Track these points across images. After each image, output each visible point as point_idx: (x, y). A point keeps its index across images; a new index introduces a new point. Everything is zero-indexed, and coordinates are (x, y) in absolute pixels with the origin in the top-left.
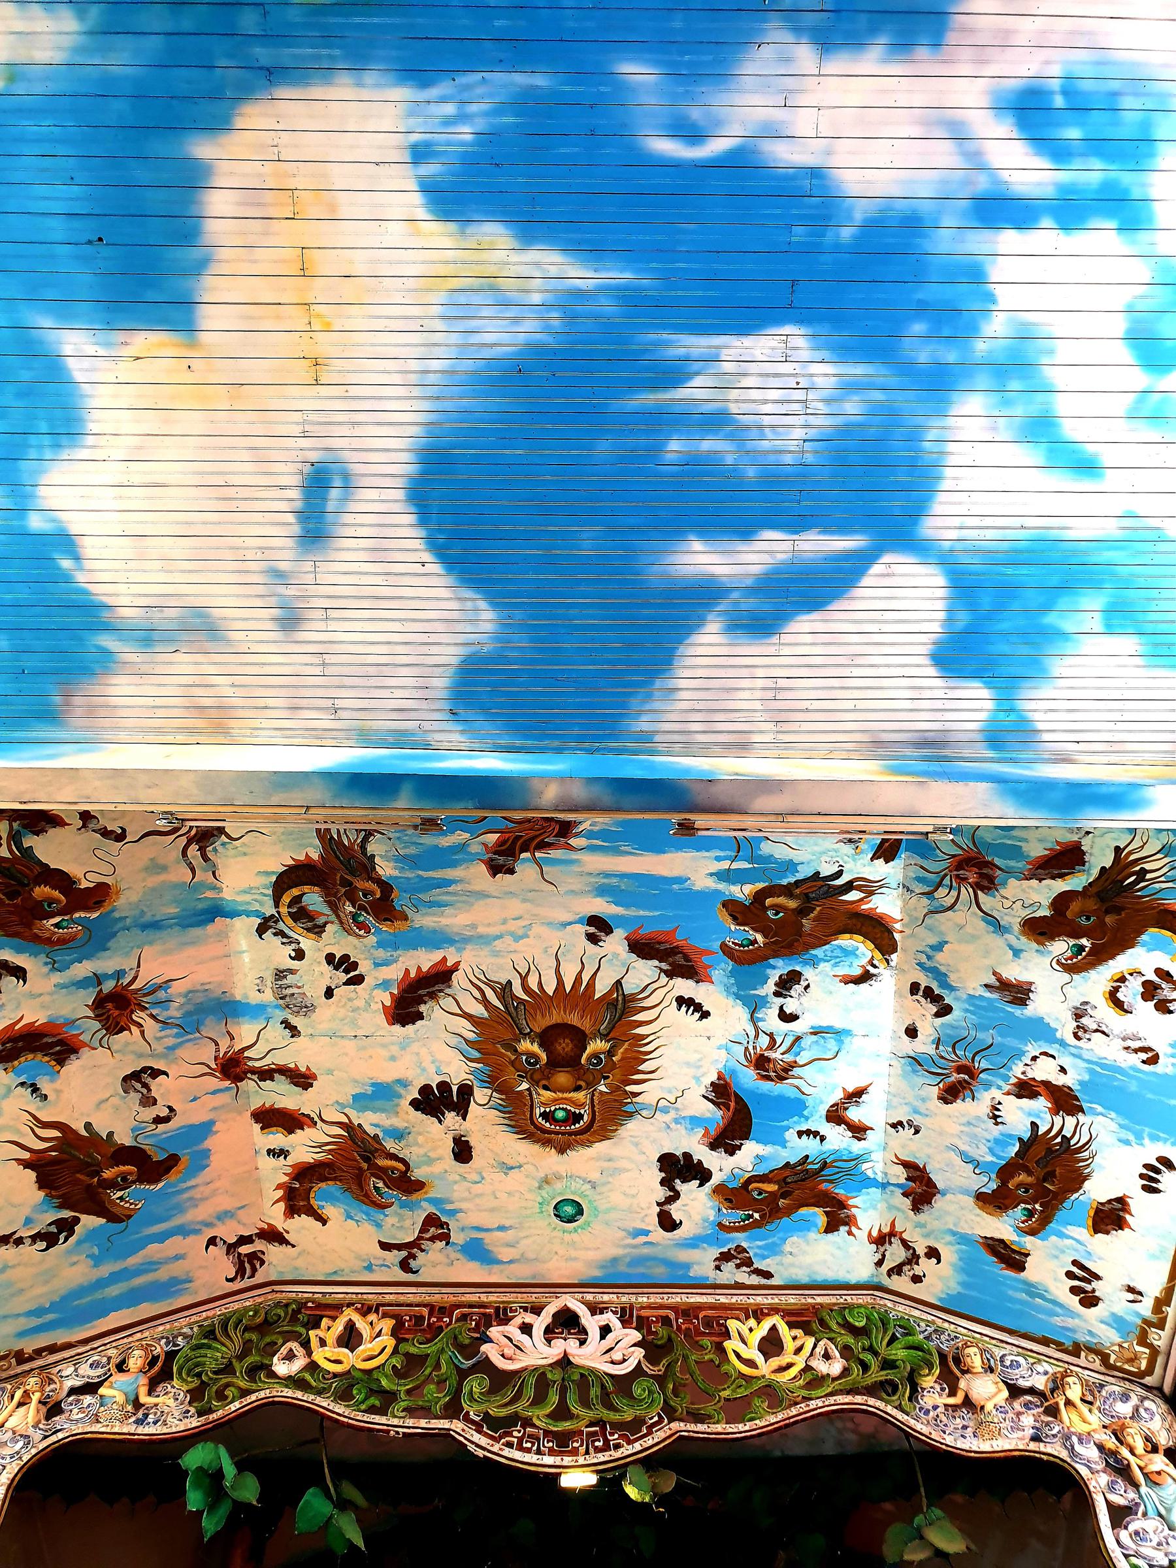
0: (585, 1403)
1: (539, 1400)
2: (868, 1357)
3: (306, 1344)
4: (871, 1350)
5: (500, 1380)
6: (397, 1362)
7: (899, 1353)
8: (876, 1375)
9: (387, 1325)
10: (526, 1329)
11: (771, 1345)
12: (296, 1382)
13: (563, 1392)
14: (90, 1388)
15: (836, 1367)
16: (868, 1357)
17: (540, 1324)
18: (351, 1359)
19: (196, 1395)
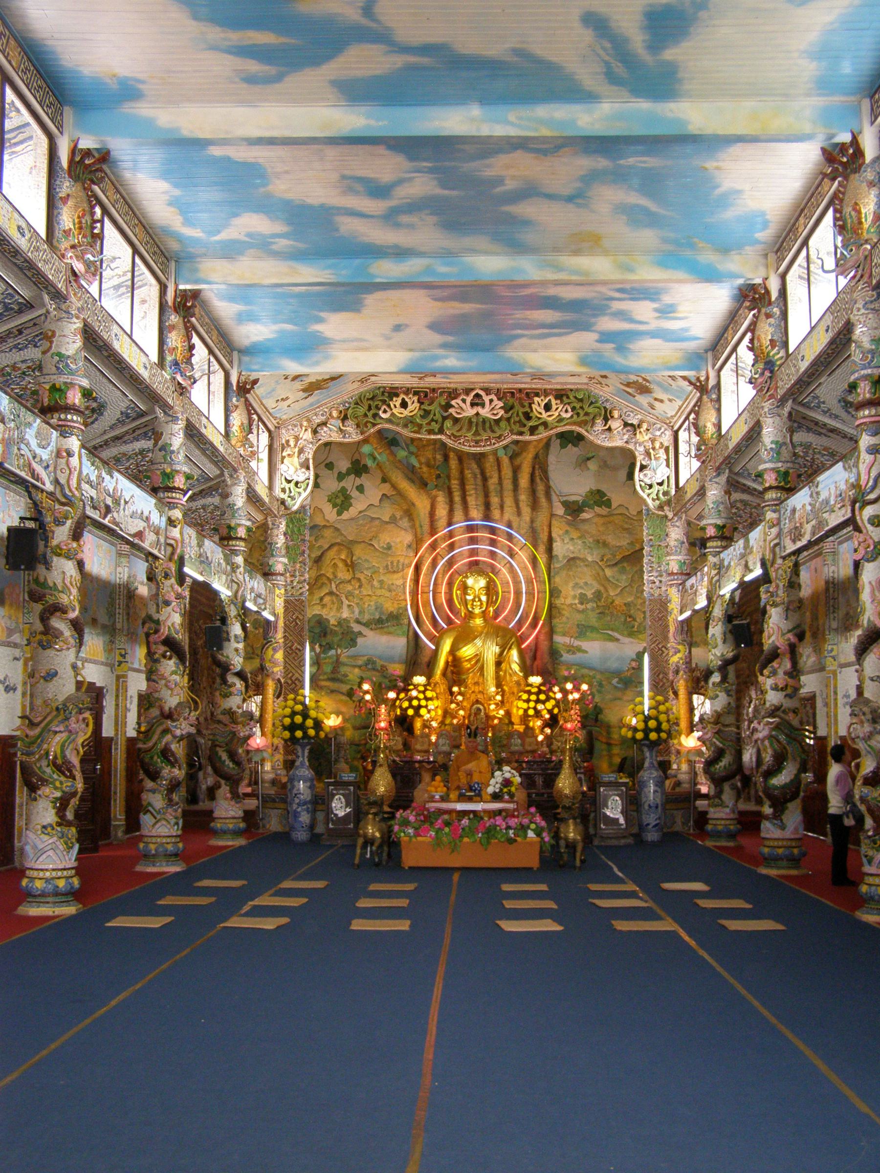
0: (484, 430)
1: (469, 430)
2: (580, 411)
3: (389, 406)
4: (582, 408)
5: (456, 421)
6: (422, 413)
7: (591, 410)
8: (582, 418)
9: (416, 398)
10: (464, 401)
11: (548, 407)
12: (389, 421)
13: (477, 425)
14: (324, 424)
15: (569, 415)
16: (580, 411)
17: (469, 399)
18: (406, 413)
19: (358, 426)
